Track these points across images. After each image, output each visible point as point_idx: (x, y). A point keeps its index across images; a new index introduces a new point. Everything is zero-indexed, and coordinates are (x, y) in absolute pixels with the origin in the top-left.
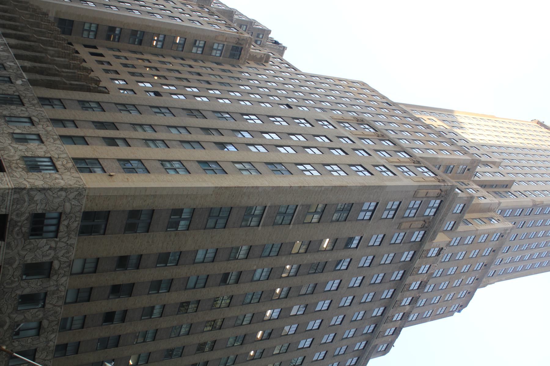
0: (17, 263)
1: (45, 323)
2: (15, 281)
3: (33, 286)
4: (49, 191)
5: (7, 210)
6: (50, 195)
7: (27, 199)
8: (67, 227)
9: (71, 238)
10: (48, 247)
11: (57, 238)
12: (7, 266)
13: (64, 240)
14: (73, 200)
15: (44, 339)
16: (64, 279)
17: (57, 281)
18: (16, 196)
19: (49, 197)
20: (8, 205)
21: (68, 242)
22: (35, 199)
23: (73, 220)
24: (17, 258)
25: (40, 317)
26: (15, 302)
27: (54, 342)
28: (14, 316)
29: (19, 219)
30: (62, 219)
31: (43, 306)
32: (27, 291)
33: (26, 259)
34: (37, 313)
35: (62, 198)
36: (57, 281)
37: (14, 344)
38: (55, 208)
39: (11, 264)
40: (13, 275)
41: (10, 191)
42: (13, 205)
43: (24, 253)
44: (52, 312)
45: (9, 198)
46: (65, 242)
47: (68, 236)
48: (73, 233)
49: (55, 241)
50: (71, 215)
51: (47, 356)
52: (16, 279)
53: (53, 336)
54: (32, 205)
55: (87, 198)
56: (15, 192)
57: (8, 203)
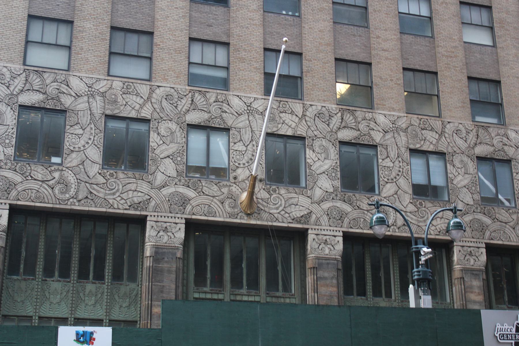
1: (194, 117)
2: (61, 176)
3: (83, 142)
12: (14, 193)
15: (244, 117)
16: (75, 82)
17: (78, 96)
25: (173, 126)
26: (121, 175)
28: (160, 178)
31: (146, 121)
32: (95, 154)
34: (163, 132)
36: (78, 96)
37: (240, 178)
40: (43, 181)
44: (165, 103)
51: (292, 113)
52: (57, 175)
53: (235, 102)
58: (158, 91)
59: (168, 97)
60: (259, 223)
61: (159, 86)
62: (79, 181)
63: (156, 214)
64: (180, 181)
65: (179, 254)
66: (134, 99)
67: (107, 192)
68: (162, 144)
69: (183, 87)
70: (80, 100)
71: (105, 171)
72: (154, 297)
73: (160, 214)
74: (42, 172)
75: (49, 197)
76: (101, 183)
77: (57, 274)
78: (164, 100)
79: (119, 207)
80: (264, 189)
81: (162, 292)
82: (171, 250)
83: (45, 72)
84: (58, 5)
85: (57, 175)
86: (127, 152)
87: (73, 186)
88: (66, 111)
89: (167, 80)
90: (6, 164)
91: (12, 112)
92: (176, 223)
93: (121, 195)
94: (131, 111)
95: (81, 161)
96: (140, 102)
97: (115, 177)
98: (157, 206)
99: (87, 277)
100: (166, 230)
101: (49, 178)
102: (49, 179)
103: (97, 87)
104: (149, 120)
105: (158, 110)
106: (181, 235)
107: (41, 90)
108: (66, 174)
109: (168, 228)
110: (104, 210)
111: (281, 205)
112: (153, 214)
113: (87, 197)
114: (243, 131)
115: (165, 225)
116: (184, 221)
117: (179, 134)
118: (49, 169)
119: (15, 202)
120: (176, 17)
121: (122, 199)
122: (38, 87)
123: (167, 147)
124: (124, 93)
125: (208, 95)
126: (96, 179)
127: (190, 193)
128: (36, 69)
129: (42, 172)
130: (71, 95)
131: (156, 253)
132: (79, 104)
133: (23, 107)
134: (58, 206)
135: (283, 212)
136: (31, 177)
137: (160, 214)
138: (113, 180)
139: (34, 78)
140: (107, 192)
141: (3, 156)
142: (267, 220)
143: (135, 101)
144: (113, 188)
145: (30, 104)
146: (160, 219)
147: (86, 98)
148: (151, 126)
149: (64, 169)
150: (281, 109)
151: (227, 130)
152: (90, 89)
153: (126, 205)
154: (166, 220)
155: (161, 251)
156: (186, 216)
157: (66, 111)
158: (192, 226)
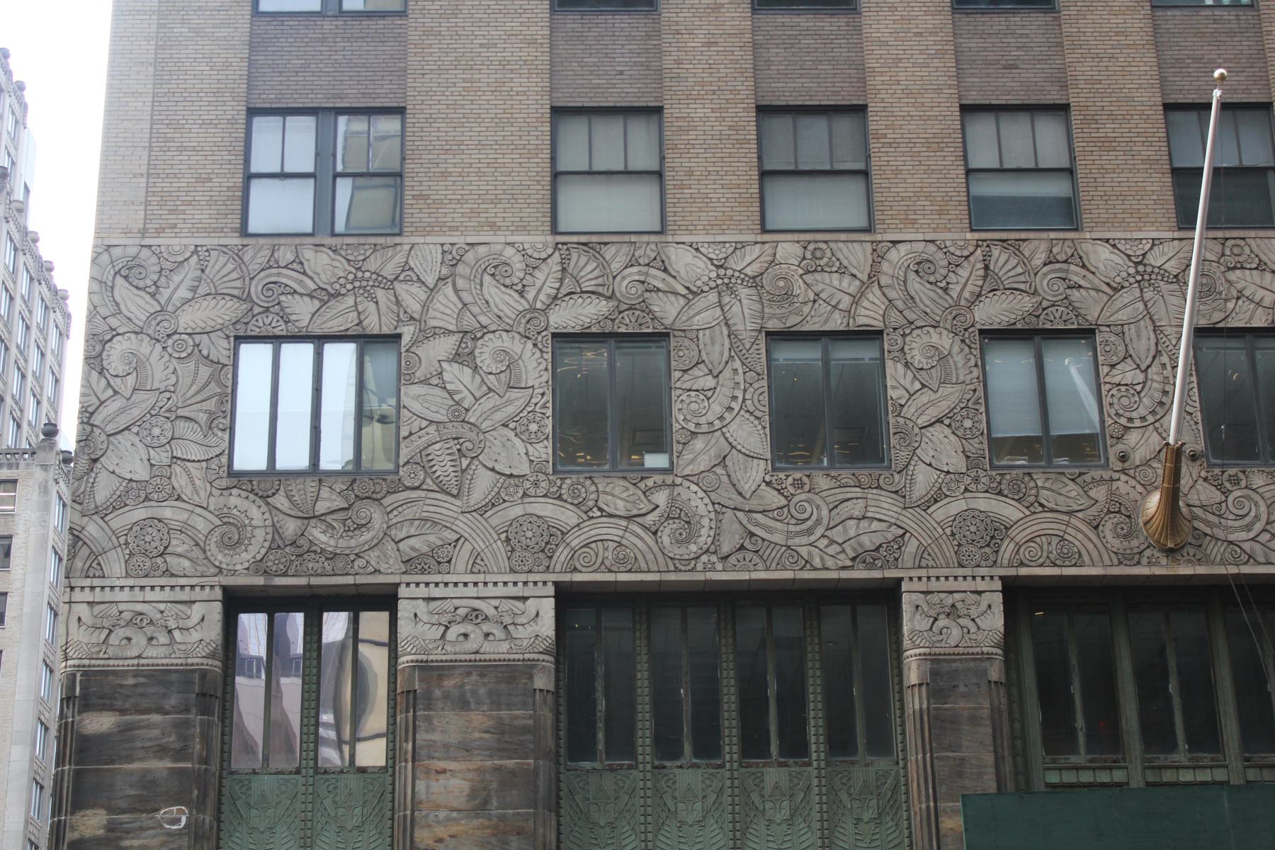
0: (547, 509)
1: (994, 312)
2: (672, 500)
3: (717, 409)
4: (97, 420)
5: (197, 594)
6: (122, 410)
7: (140, 514)
8: (337, 295)
9: (406, 267)
10: (458, 376)
11: (399, 336)
12: (562, 555)
13: (412, 297)
14: (165, 294)
17: (693, 293)
18: (115, 565)
19: (136, 413)
20: (167, 595)
21: (430, 281)
22: (142, 473)
23: (289, 278)
24: (517, 511)
25: (944, 340)
26: (822, 482)
27: (1155, 242)
28: (923, 480)
29: (260, 534)
30: (281, 329)
31: (872, 335)
32: (752, 435)
33: (524, 469)
34: (918, 358)
35: (145, 347)
36: (693, 293)
37: (1137, 457)
38: (205, 372)
39: (553, 536)
40: (629, 518)
41: (77, 596)
42: (168, 573)
43: (483, 483)
44: (915, 284)
45: (125, 595)
46: (432, 290)
47: (389, 284)
48: (372, 265)
49: (415, 342)
50: (255, 289)
52: (661, 498)
53: (1102, 257)
54: (180, 480)
55: (160, 231)
56: (94, 569)
57: (149, 595)
58: (893, 255)
59: (921, 266)
60: (1201, 570)
61: (894, 243)
62: (719, 508)
63: (923, 573)
64: (976, 480)
65: (995, 672)
66: (836, 283)
67: (792, 528)
68: (917, 391)
69: (959, 236)
70: (701, 303)
71: (782, 475)
72: (942, 790)
73: (933, 572)
74: (624, 495)
75: (650, 557)
76: (774, 506)
77: (687, 748)
78: (912, 276)
79: (826, 561)
80: (1205, 479)
81: (960, 775)
82: (972, 664)
83: (606, 244)
84: (621, 73)
85: (661, 498)
86: (832, 420)
87: (705, 522)
88: (667, 335)
89: (914, 222)
90: (536, 484)
91: (538, 354)
92: (979, 593)
93: (828, 533)
94: (831, 313)
95: (717, 456)
96: (852, 290)
97: (807, 488)
98: (923, 551)
99: (764, 752)
100: (953, 612)
101: (645, 506)
102: (643, 511)
103: (736, 264)
104: (880, 333)
105: (900, 304)
106: (995, 621)
107: (600, 290)
108: (685, 494)
109: (959, 605)
110: (788, 575)
111: (1257, 518)
112: (913, 573)
113: (742, 547)
114: (1131, 332)
115: (949, 600)
116: (998, 585)
117: (960, 360)
118: (642, 485)
119: (567, 578)
120: (920, 59)
121: (832, 542)
122: (593, 282)
123: (933, 396)
124: (808, 272)
125: (1026, 249)
126: (761, 497)
127: (1008, 510)
128: (583, 239)
129: (624, 495)
130: (676, 294)
131: (935, 674)
132: (698, 313)
133: (561, 338)
134: (673, 577)
135: (1265, 537)
136: (600, 509)
137: (933, 572)
138: (803, 497)
139: (582, 263)
140: (792, 528)
141: (527, 465)
142: (1223, 562)
143: (837, 287)
144: (805, 516)
145: (578, 329)
146: (934, 585)
147: (713, 297)
148: (886, 347)
149: (678, 481)
150: (1231, 261)
151: (1086, 334)
152: (722, 272)
153: (842, 556)
154: (952, 584)
155: (945, 667)
156: (1003, 572)
157: (667, 335)
158: (1020, 596)
